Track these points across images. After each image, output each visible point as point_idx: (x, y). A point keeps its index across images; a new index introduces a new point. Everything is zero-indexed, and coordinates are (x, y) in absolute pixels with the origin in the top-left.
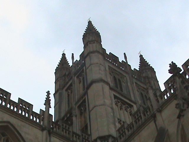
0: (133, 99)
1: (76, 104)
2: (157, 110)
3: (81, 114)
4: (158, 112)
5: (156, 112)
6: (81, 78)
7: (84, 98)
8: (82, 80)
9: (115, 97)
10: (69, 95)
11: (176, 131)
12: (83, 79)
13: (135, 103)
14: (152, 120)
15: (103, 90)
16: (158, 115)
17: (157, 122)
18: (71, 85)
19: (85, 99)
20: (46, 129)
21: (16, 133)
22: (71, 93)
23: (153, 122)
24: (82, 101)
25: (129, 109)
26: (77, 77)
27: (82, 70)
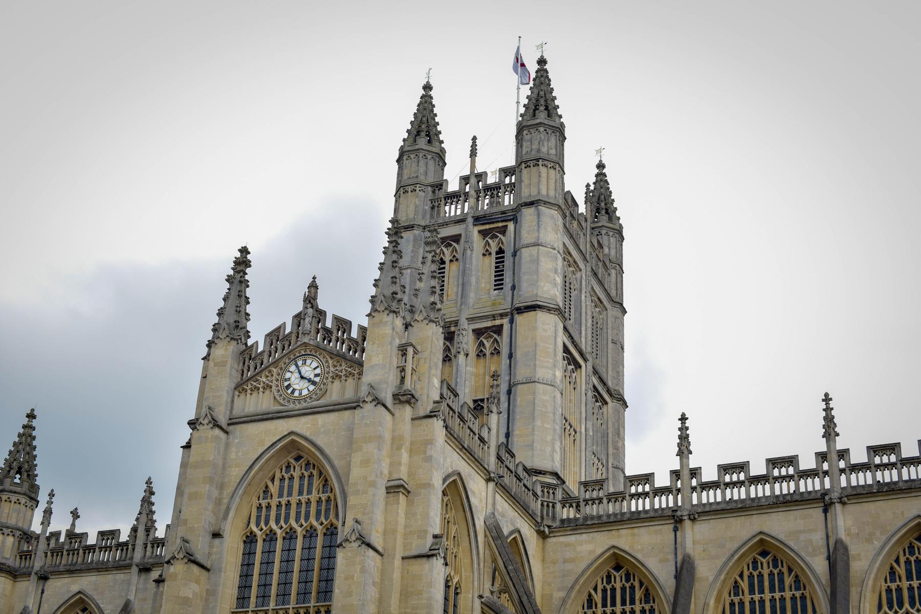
0: (583, 347)
1: (471, 320)
2: (689, 515)
3: (480, 354)
4: (690, 519)
5: (685, 518)
6: (494, 248)
7: (498, 322)
8: (494, 255)
9: (566, 350)
11: (711, 578)
12: (501, 251)
13: (585, 360)
14: (669, 522)
15: (556, 338)
16: (687, 523)
17: (678, 533)
18: (457, 238)
19: (502, 325)
20: (494, 481)
21: (464, 496)
22: (451, 261)
23: (671, 527)
24: (489, 324)
25: (574, 375)
26: (483, 233)
27: (500, 225)
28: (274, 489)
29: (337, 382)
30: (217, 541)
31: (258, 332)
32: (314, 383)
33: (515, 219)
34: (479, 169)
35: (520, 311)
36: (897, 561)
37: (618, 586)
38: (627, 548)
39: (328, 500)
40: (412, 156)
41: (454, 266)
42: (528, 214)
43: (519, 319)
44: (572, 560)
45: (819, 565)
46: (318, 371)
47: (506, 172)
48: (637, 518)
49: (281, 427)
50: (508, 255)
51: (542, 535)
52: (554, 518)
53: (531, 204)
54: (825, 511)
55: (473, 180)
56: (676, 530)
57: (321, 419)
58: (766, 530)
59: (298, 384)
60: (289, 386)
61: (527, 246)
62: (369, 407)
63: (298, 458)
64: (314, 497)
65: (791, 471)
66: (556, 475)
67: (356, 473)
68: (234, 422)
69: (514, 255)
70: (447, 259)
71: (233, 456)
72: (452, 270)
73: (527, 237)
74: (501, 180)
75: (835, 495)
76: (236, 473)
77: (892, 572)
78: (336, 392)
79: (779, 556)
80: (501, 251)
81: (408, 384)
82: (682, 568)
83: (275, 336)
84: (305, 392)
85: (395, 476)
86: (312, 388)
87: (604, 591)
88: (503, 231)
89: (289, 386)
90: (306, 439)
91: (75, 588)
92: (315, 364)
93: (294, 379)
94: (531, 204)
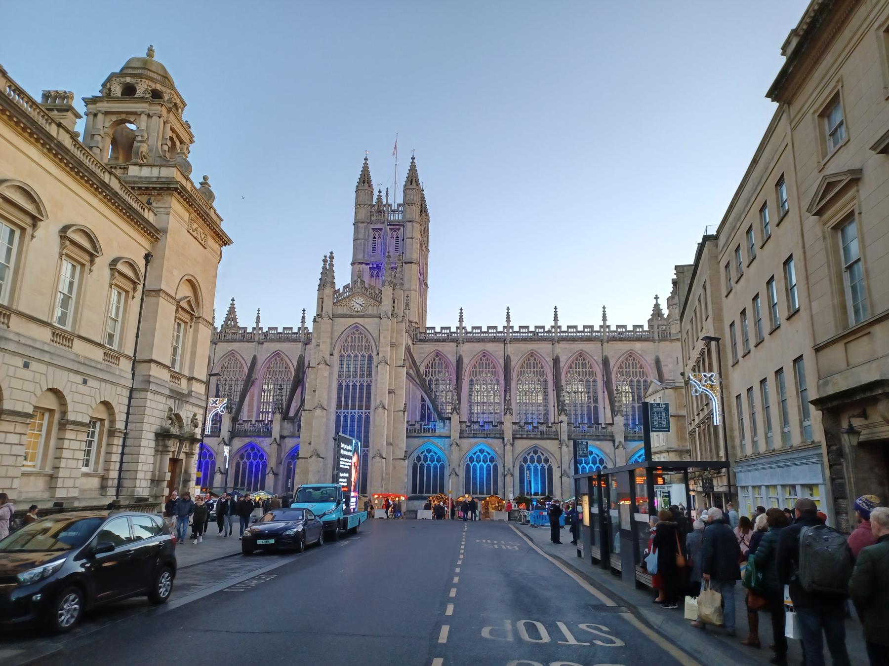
6: (395, 236)
10: (375, 238)
12: (397, 237)
18: (381, 229)
28: (349, 340)
29: (370, 307)
30: (332, 356)
31: (339, 286)
32: (362, 306)
33: (404, 227)
34: (389, 203)
35: (405, 263)
36: (524, 362)
37: (437, 362)
38: (441, 350)
39: (369, 346)
40: (363, 192)
41: (380, 240)
42: (409, 224)
43: (406, 266)
44: (422, 353)
45: (502, 362)
46: (363, 302)
47: (399, 205)
48: (444, 340)
49: (352, 321)
50: (400, 239)
51: (413, 344)
52: (417, 339)
53: (410, 221)
54: (505, 345)
55: (387, 206)
56: (457, 346)
57: (366, 319)
58: (486, 349)
59: (356, 306)
60: (353, 306)
61: (409, 238)
62: (385, 319)
63: (357, 330)
64: (364, 344)
65: (495, 331)
66: (417, 323)
67: (382, 340)
68: (334, 316)
69: (403, 240)
70: (377, 237)
71: (335, 328)
72: (379, 242)
73: (408, 234)
74: (398, 209)
75: (508, 341)
76: (337, 334)
77: (522, 365)
78: (370, 311)
79: (489, 358)
80: (397, 237)
81: (395, 312)
82: (459, 359)
83: (345, 287)
84: (359, 309)
85: (393, 341)
86: (362, 308)
87: (432, 363)
88: (399, 229)
89: (353, 306)
90: (362, 325)
91: (230, 349)
92: (362, 300)
93: (355, 304)
94: (410, 221)
